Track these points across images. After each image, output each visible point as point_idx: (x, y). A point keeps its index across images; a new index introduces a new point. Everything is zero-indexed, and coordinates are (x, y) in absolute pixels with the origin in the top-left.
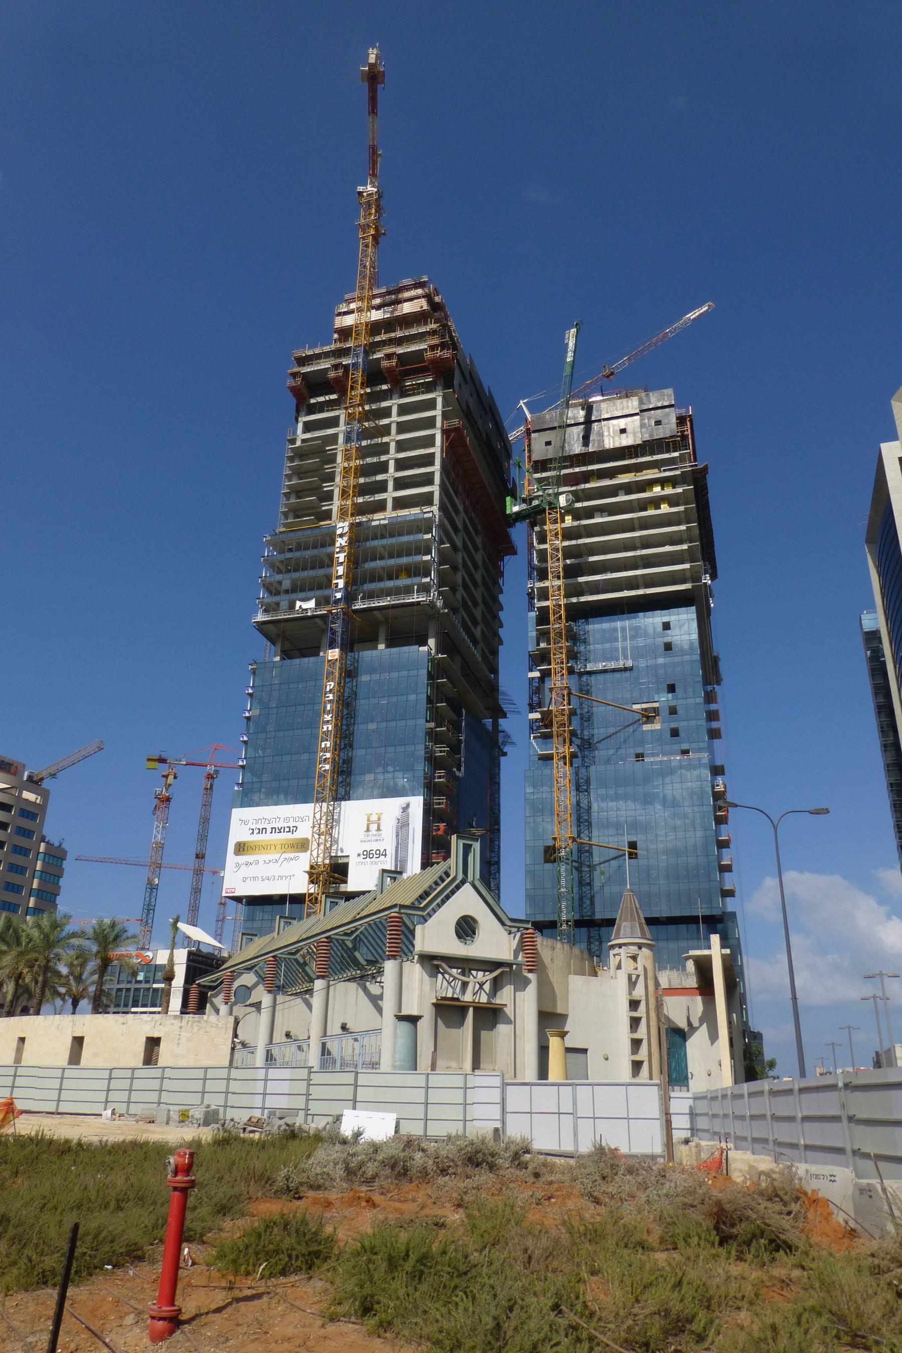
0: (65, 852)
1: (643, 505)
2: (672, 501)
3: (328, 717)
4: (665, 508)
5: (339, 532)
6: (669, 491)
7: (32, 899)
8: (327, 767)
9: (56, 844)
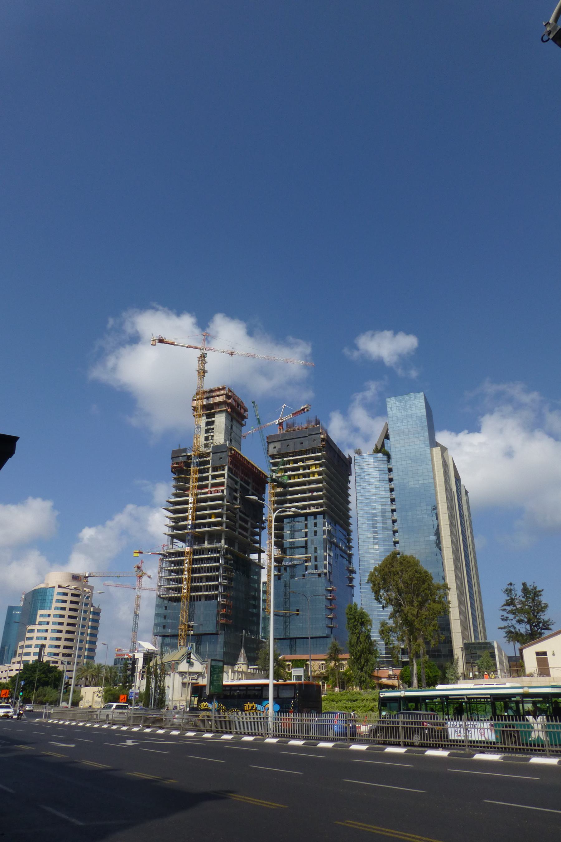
0: (100, 610)
1: (308, 475)
2: (319, 474)
3: (186, 573)
4: (316, 477)
5: (190, 502)
6: (319, 469)
7: (89, 630)
8: (186, 591)
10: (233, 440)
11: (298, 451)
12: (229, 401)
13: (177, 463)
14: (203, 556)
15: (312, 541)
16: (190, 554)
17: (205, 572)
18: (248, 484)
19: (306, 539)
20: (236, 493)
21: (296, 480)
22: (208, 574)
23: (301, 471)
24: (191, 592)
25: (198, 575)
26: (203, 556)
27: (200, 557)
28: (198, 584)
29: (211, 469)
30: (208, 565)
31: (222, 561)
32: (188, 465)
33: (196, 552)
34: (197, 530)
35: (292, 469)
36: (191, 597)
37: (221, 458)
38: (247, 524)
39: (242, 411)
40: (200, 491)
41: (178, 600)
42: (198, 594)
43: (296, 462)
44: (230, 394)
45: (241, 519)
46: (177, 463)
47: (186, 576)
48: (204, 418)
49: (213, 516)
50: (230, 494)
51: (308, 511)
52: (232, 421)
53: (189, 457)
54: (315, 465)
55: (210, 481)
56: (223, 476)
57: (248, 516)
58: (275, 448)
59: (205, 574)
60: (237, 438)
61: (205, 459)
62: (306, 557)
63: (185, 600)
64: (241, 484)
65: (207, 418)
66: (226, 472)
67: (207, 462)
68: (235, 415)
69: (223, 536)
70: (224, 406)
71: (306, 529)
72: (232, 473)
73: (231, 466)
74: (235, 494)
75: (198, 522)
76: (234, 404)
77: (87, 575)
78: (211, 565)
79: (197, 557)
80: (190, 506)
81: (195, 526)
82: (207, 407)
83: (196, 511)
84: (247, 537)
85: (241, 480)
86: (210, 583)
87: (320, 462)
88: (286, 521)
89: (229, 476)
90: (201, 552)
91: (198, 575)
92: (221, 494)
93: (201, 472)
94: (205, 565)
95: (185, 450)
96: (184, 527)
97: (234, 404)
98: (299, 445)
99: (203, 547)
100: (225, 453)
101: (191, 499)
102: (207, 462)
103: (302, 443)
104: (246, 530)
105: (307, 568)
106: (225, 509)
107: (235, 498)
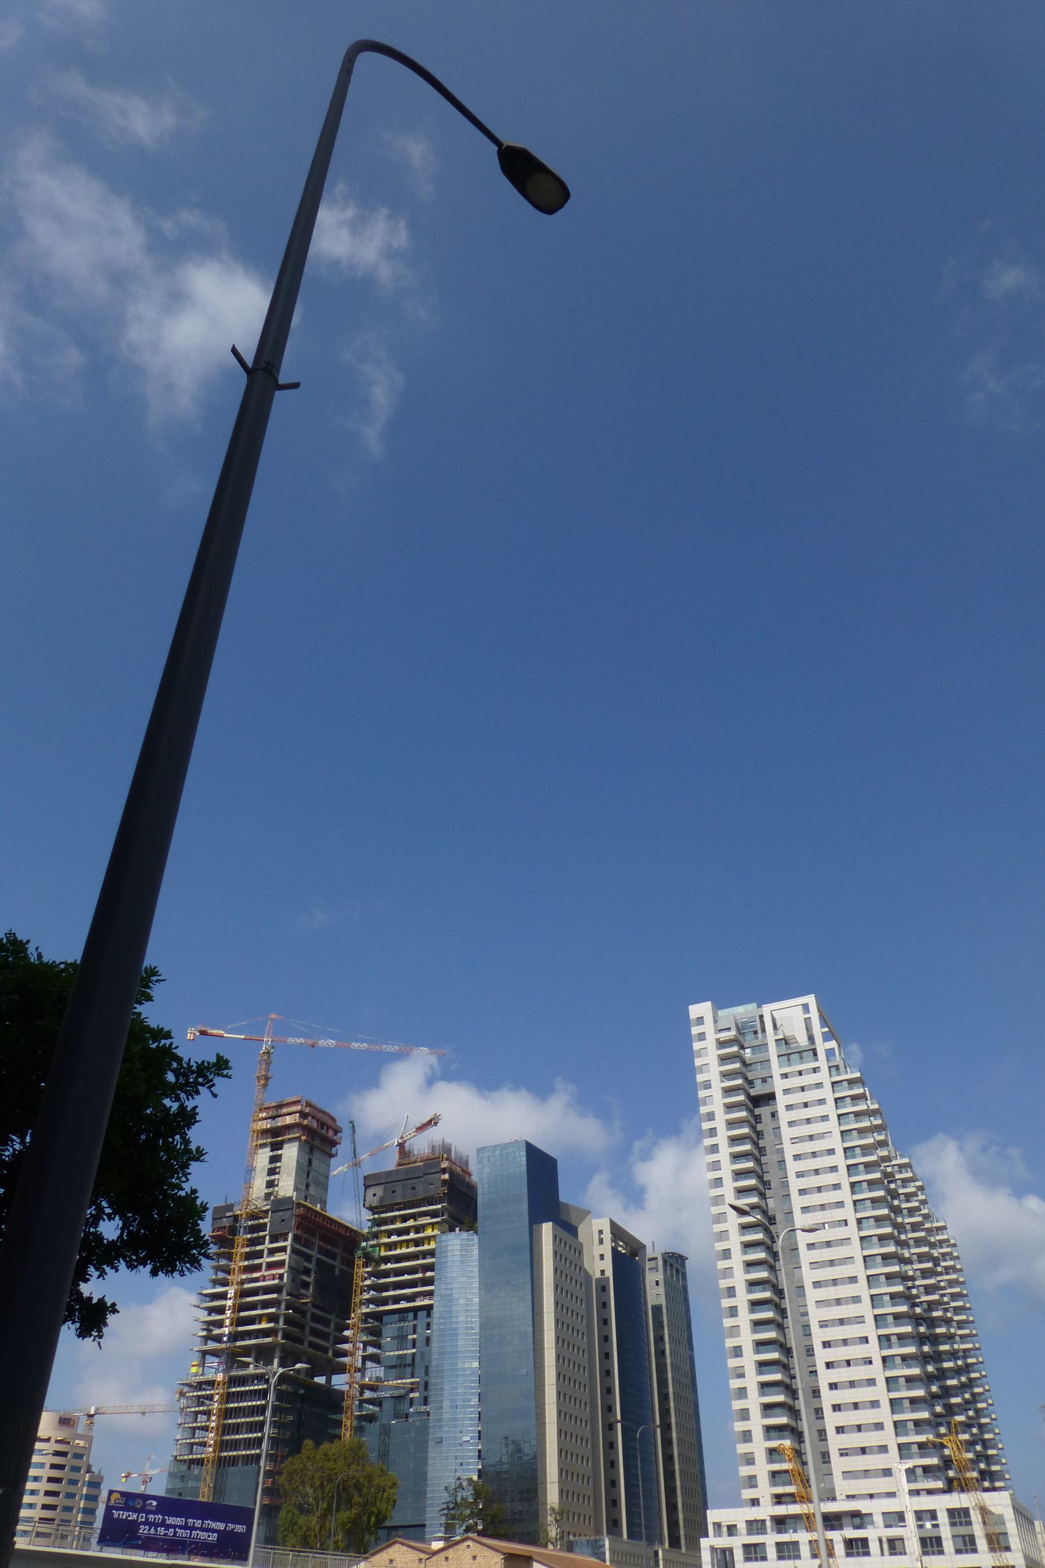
0: (102, 1478)
3: (214, 1418)
9: (97, 1473)
10: (312, 1185)
11: (409, 1202)
12: (306, 1122)
13: (219, 1229)
14: (243, 1389)
15: (423, 1354)
16: (224, 1384)
17: (244, 1417)
18: (332, 1256)
19: (414, 1351)
20: (309, 1275)
21: (404, 1250)
22: (248, 1420)
23: (412, 1236)
24: (221, 1451)
25: (234, 1421)
26: (243, 1389)
27: (238, 1389)
28: (232, 1437)
29: (267, 1238)
30: (250, 1404)
31: (271, 1397)
32: (233, 1230)
33: (233, 1381)
34: (238, 1343)
35: (400, 1232)
36: (220, 1458)
37: (283, 1221)
38: (329, 1327)
39: (331, 1133)
40: (249, 1276)
41: (200, 1462)
42: (230, 1454)
43: (405, 1219)
44: (307, 1110)
45: (316, 1318)
46: (219, 1229)
47: (213, 1424)
48: (268, 1149)
49: (264, 1319)
50: (293, 1280)
51: (418, 1303)
52: (311, 1151)
53: (236, 1218)
54: (433, 1224)
55: (267, 1259)
56: (283, 1249)
57: (330, 1313)
58: (374, 1195)
59: (243, 1420)
60: (321, 1179)
61: (261, 1221)
62: (412, 1383)
63: (210, 1466)
64: (318, 1260)
65: (272, 1150)
66: (288, 1243)
67: (262, 1227)
68: (317, 1143)
69: (278, 1354)
70: (296, 1130)
71: (414, 1333)
72: (300, 1244)
73: (299, 1233)
74: (305, 1278)
75: (240, 1329)
76: (315, 1124)
77: (92, 1412)
78: (254, 1403)
79: (234, 1390)
80: (229, 1303)
81: (234, 1337)
82: (275, 1132)
83: (239, 1311)
84: (325, 1350)
85: (320, 1252)
86: (250, 1436)
87: (439, 1219)
88: (386, 1319)
89: (294, 1251)
90: (242, 1381)
91: (234, 1421)
92: (276, 1281)
93: (253, 1242)
94: (245, 1404)
95: (230, 1208)
96: (218, 1339)
97: (315, 1124)
98: (409, 1191)
99: (245, 1372)
100: (289, 1212)
101: (231, 1292)
102: (262, 1227)
103: (414, 1188)
104: (325, 1336)
105: (411, 1405)
106: (283, 1306)
107: (305, 1285)
